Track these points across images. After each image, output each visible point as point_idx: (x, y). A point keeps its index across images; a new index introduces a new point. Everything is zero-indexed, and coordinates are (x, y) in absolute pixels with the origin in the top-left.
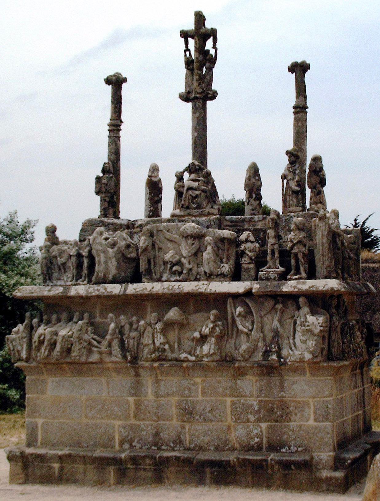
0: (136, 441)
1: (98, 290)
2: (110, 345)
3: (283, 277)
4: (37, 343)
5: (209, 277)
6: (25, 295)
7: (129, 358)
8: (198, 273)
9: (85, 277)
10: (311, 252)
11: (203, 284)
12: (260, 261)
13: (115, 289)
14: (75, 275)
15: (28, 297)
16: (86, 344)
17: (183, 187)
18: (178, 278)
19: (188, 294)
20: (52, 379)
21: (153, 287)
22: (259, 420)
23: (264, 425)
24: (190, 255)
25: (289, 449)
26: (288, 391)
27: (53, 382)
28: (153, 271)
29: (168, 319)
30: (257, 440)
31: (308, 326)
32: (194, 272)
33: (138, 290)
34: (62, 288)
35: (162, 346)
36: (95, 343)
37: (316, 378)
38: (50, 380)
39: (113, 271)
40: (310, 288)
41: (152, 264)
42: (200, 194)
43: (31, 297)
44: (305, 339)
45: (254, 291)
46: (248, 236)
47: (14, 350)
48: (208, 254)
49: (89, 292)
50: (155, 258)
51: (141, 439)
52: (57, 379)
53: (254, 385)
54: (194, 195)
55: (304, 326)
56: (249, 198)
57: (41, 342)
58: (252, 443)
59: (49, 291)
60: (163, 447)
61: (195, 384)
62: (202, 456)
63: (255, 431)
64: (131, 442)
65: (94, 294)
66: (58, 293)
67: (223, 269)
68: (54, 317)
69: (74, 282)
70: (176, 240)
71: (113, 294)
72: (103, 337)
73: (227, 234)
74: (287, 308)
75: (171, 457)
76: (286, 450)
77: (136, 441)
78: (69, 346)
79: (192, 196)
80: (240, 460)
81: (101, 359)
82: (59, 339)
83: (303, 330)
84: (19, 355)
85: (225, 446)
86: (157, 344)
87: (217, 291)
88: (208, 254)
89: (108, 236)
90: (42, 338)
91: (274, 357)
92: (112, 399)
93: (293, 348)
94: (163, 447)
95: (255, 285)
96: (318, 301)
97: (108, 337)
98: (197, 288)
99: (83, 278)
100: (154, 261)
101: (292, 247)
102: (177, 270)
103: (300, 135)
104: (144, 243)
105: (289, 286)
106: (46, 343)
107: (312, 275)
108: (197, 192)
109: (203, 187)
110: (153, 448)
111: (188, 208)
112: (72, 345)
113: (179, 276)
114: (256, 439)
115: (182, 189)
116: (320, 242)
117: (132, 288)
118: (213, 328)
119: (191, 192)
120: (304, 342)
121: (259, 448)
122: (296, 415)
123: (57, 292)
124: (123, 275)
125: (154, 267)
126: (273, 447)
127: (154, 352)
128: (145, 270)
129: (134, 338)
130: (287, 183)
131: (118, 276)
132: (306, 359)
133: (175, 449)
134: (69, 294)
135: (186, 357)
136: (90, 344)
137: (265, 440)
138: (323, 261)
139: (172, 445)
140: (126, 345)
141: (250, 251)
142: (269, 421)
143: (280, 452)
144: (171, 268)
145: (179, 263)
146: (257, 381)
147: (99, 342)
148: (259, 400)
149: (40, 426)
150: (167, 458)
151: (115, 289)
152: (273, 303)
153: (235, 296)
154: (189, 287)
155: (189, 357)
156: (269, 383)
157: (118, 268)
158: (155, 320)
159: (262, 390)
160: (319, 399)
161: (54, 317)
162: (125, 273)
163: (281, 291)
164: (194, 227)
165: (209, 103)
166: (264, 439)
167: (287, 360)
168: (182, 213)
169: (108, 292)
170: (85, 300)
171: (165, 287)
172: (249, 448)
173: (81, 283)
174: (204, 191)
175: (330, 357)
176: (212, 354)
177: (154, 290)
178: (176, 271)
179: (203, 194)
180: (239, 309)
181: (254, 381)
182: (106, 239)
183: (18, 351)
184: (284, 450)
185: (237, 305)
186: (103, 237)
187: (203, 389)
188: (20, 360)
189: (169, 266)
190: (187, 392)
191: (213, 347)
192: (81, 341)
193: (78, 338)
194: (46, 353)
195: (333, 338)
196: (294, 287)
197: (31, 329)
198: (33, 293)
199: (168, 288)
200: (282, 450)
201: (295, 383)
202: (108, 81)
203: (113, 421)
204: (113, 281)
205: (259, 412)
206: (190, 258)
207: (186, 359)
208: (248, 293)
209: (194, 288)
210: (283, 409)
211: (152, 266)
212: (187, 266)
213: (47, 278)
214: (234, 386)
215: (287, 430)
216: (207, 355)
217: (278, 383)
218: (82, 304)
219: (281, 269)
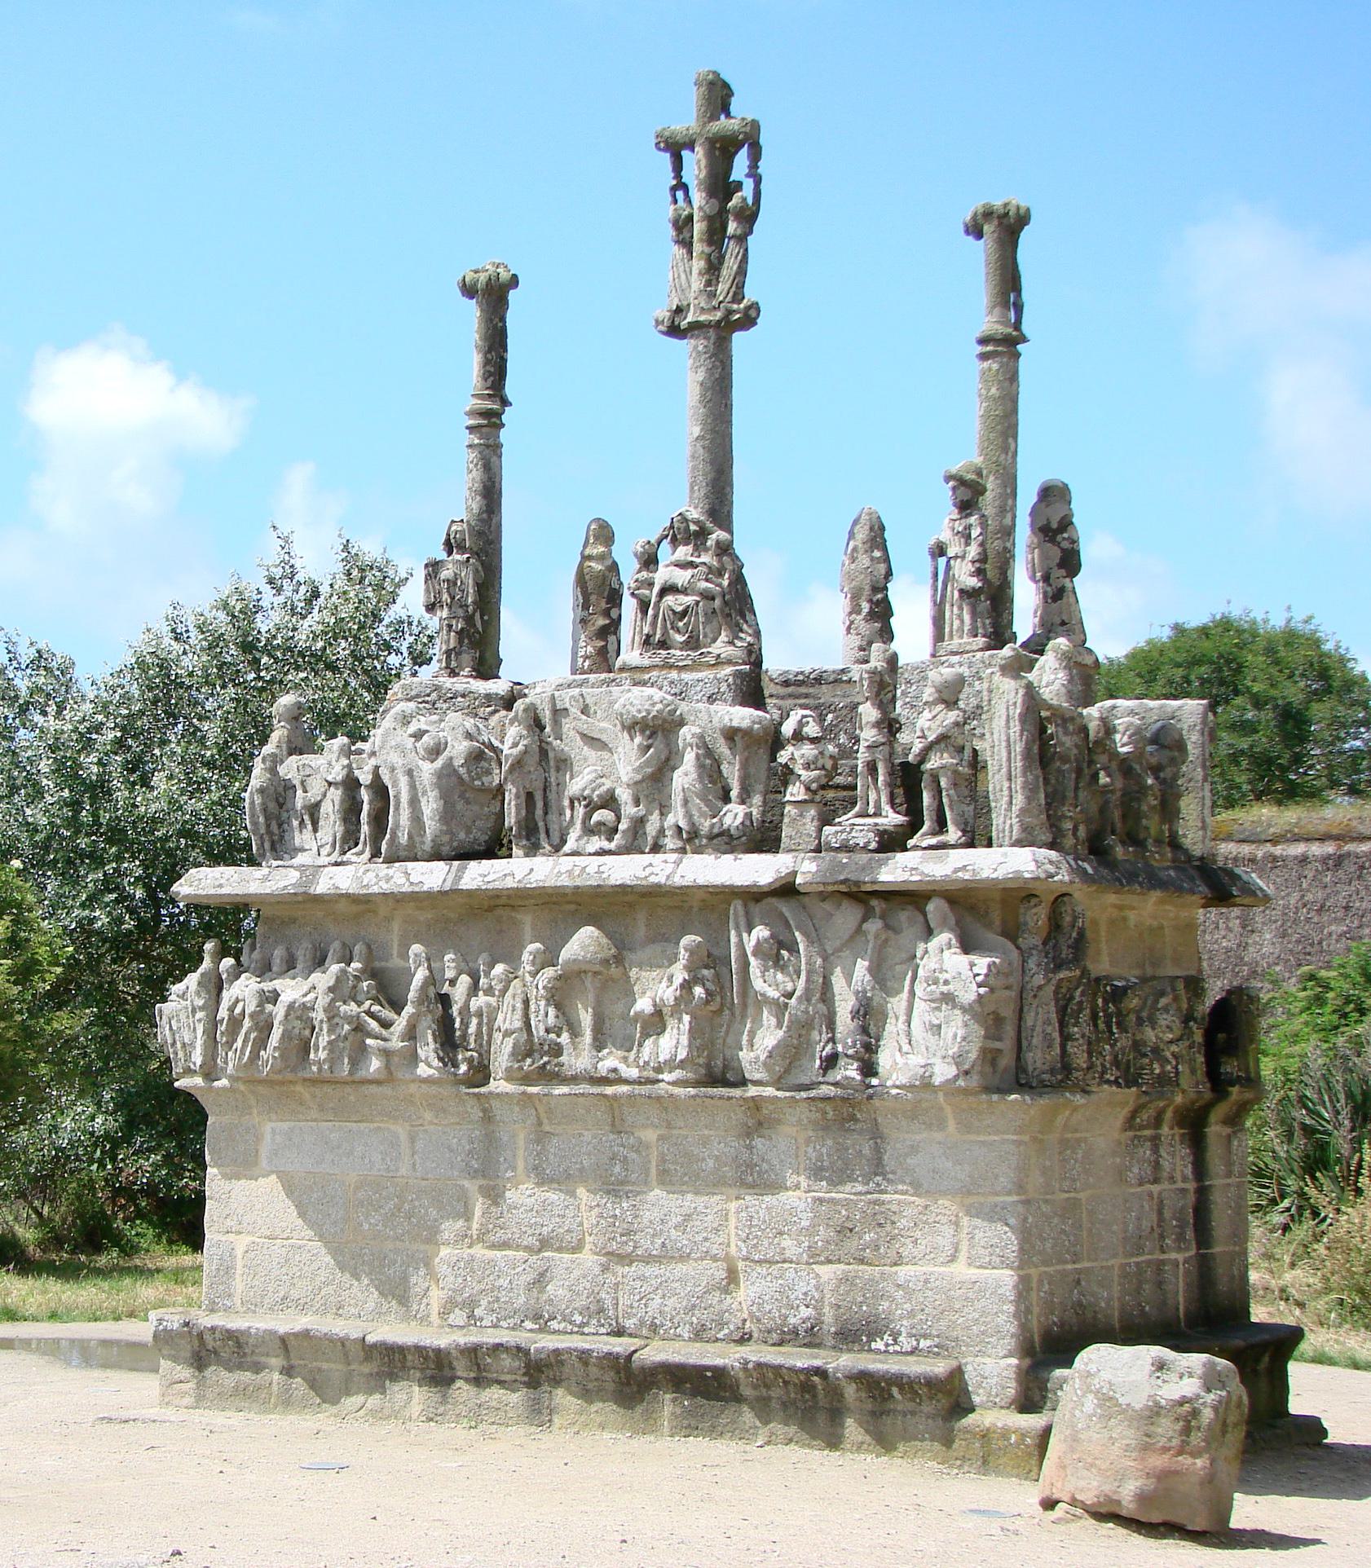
0: (484, 1303)
2: (411, 1034)
3: (892, 842)
5: (692, 840)
6: (201, 892)
8: (661, 832)
9: (365, 843)
10: (976, 764)
12: (833, 797)
13: (432, 876)
14: (339, 836)
16: (347, 1027)
17: (651, 585)
18: (606, 845)
19: (623, 889)
20: (273, 1125)
22: (815, 1257)
23: (827, 1272)
24: (639, 777)
25: (895, 1340)
26: (894, 1173)
27: (273, 1130)
28: (541, 824)
29: (567, 962)
30: (805, 1312)
31: (946, 982)
32: (651, 829)
34: (297, 874)
35: (553, 1036)
37: (973, 1137)
38: (268, 1127)
39: (431, 825)
40: (956, 871)
41: (540, 804)
42: (697, 603)
44: (937, 1022)
45: (798, 881)
46: (801, 724)
47: (174, 1043)
48: (684, 777)
51: (497, 1300)
52: (285, 1125)
53: (801, 1153)
54: (680, 609)
55: (935, 983)
56: (850, 613)
57: (235, 1023)
58: (792, 1320)
59: (265, 879)
60: (554, 1325)
61: (640, 1147)
62: (655, 1353)
63: (801, 1287)
64: (471, 1304)
65: (376, 889)
67: (728, 821)
68: (278, 954)
69: (335, 857)
70: (604, 738)
71: (425, 888)
72: (398, 1007)
73: (743, 719)
74: (897, 931)
75: (569, 1351)
76: (887, 1345)
77: (484, 1303)
78: (307, 1032)
80: (750, 1366)
82: (279, 1011)
83: (932, 992)
85: (722, 1325)
86: (539, 1031)
87: (701, 881)
89: (424, 727)
90: (238, 1010)
91: (850, 1071)
92: (424, 1183)
93: (906, 1048)
94: (554, 1325)
95: (807, 862)
96: (974, 912)
97: (409, 1009)
98: (649, 870)
99: (360, 846)
101: (924, 756)
103: (1004, 424)
104: (515, 745)
105: (898, 870)
107: (977, 836)
108: (689, 600)
109: (704, 585)
110: (528, 1324)
111: (664, 644)
113: (610, 840)
114: (803, 1308)
115: (647, 592)
116: (1004, 738)
117: (479, 874)
118: (687, 986)
119: (669, 600)
120: (937, 1029)
121: (811, 1337)
122: (915, 1242)
123: (282, 884)
124: (462, 835)
125: (546, 813)
126: (851, 1335)
127: (529, 1053)
128: (518, 822)
130: (948, 567)
131: (446, 839)
132: (937, 1080)
133: (586, 1330)
134: (312, 891)
135: (615, 1070)
136: (359, 1029)
137: (828, 1315)
138: (1008, 793)
139: (578, 1319)
140: (458, 1033)
141: (807, 766)
142: (839, 1261)
143: (870, 1350)
144: (588, 816)
145: (610, 801)
146: (808, 1141)
148: (815, 1200)
149: (239, 1252)
150: (557, 1352)
151: (432, 876)
152: (859, 916)
153: (753, 896)
154: (626, 870)
155: (622, 1067)
156: (841, 1149)
157: (447, 815)
158: (533, 964)
159: (822, 1169)
160: (982, 1200)
162: (469, 832)
163: (874, 883)
164: (651, 697)
165: (738, 338)
166: (826, 1310)
167: (889, 1083)
168: (646, 662)
170: (362, 904)
172: (787, 1337)
173: (354, 859)
174: (708, 596)
175: (1020, 1080)
176: (682, 1061)
177: (533, 877)
178: (600, 824)
180: (761, 932)
181: (801, 1141)
182: (418, 735)
184: (878, 1345)
185: (757, 920)
186: (412, 729)
187: (663, 1160)
188: (188, 1072)
189: (580, 811)
190: (617, 1169)
191: (684, 1040)
192: (336, 1020)
195: (1030, 1023)
196: (913, 869)
197: (215, 986)
198: (221, 886)
200: (873, 1346)
201: (914, 1149)
202: (468, 290)
203: (422, 1247)
204: (436, 856)
205: (811, 1231)
206: (639, 787)
207: (612, 1076)
208: (786, 890)
210: (880, 1225)
211: (539, 812)
212: (629, 810)
213: (267, 845)
214: (746, 1156)
215: (891, 1289)
216: (671, 1064)
217: (866, 1151)
218: (357, 917)
219: (892, 818)
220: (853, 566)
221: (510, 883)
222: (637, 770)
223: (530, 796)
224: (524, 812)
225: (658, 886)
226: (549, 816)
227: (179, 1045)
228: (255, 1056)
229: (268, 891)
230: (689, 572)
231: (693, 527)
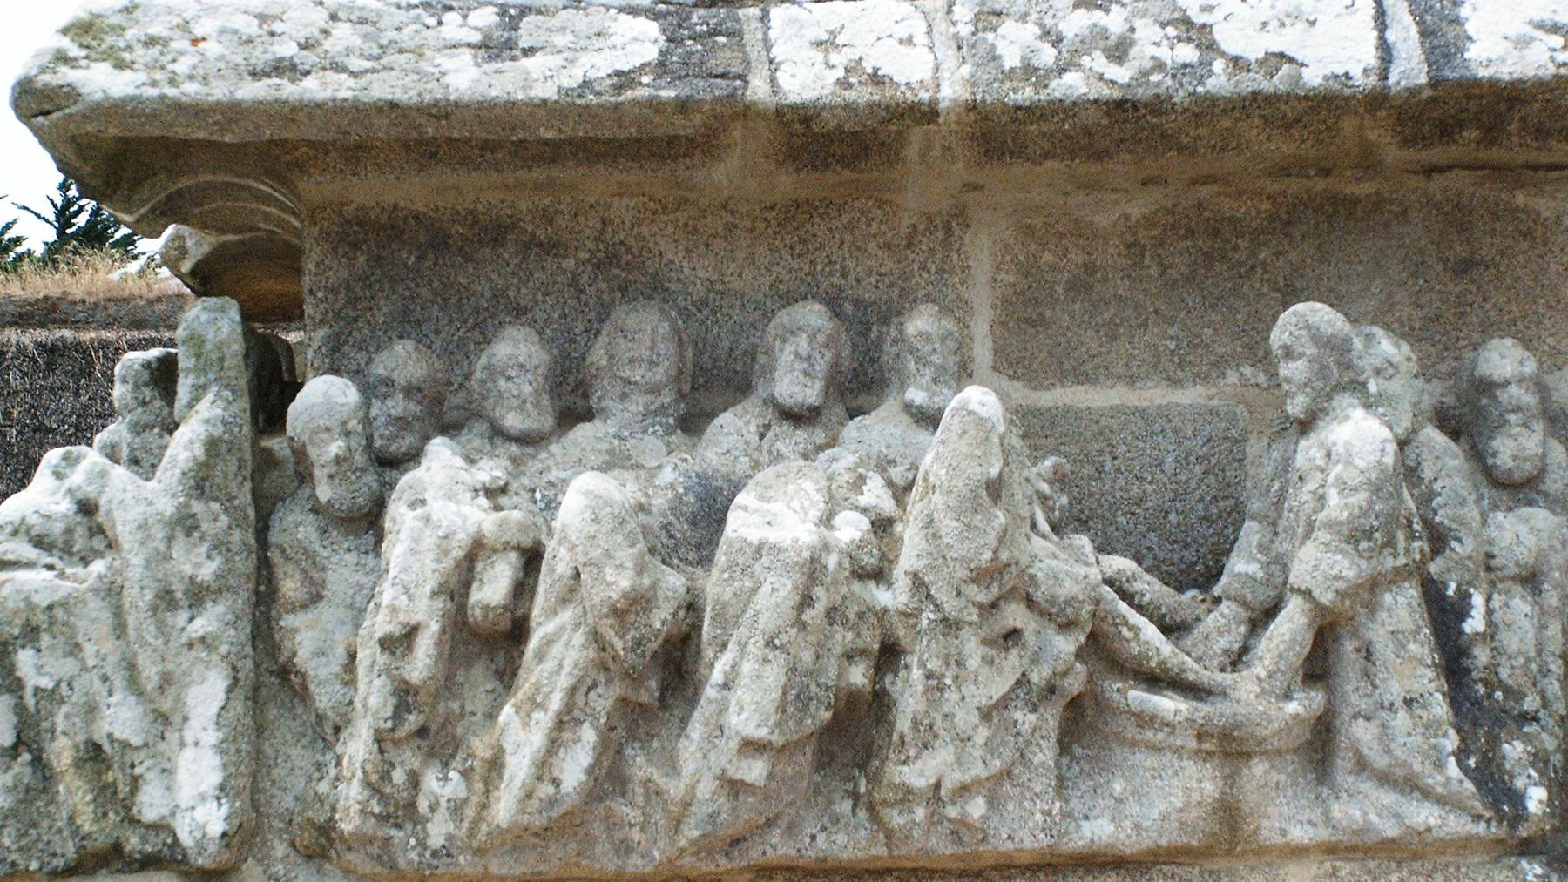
1: (1119, 51)
4: (425, 646)
6: (191, 89)
7: (1536, 798)
15: (233, 112)
34: (651, 28)
36: (1150, 632)
43: (262, 110)
49: (1011, 60)
59: (495, 48)
65: (1073, 85)
66: (624, 79)
68: (516, 352)
71: (1313, 77)
78: (858, 676)
81: (1229, 813)
84: (117, 799)
90: (493, 587)
106: (558, 649)
112: (889, 655)
123: (599, 65)
129: (1531, 580)
147: (1172, 629)
161: (516, 352)
169: (1237, 62)
183: (94, 755)
193: (981, 576)
194: (574, 769)
227: (61, 753)
228: (609, 777)
229: (548, 91)
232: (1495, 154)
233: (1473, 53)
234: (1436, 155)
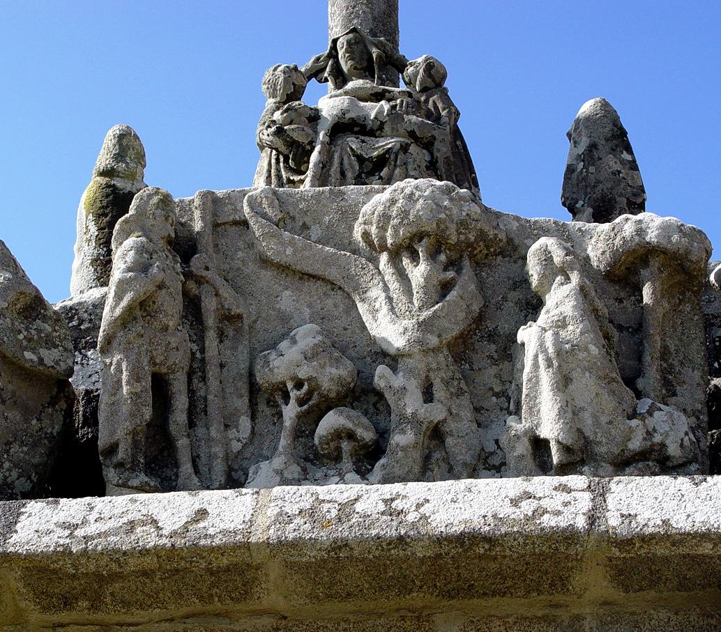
11: (566, 489)
19: (467, 541)
21: (202, 514)
28: (182, 442)
33: (92, 529)
41: (181, 402)
42: (404, 148)
50: (197, 369)
79: (360, 159)
88: (562, 323)
98: (527, 507)
100: (191, 392)
102: (352, 424)
119: (353, 143)
125: (191, 424)
171: (292, 509)
179: (413, 149)
189: (290, 411)
199: (311, 514)
209: (506, 510)
211: (179, 416)
220: (592, 169)
221: (148, 538)
222: (424, 326)
223: (160, 386)
224: (148, 413)
225: (569, 536)
226: (200, 431)
230: (385, 105)
231: (375, 52)
232: (100, 616)
233: (15, 538)
234: (64, 616)
